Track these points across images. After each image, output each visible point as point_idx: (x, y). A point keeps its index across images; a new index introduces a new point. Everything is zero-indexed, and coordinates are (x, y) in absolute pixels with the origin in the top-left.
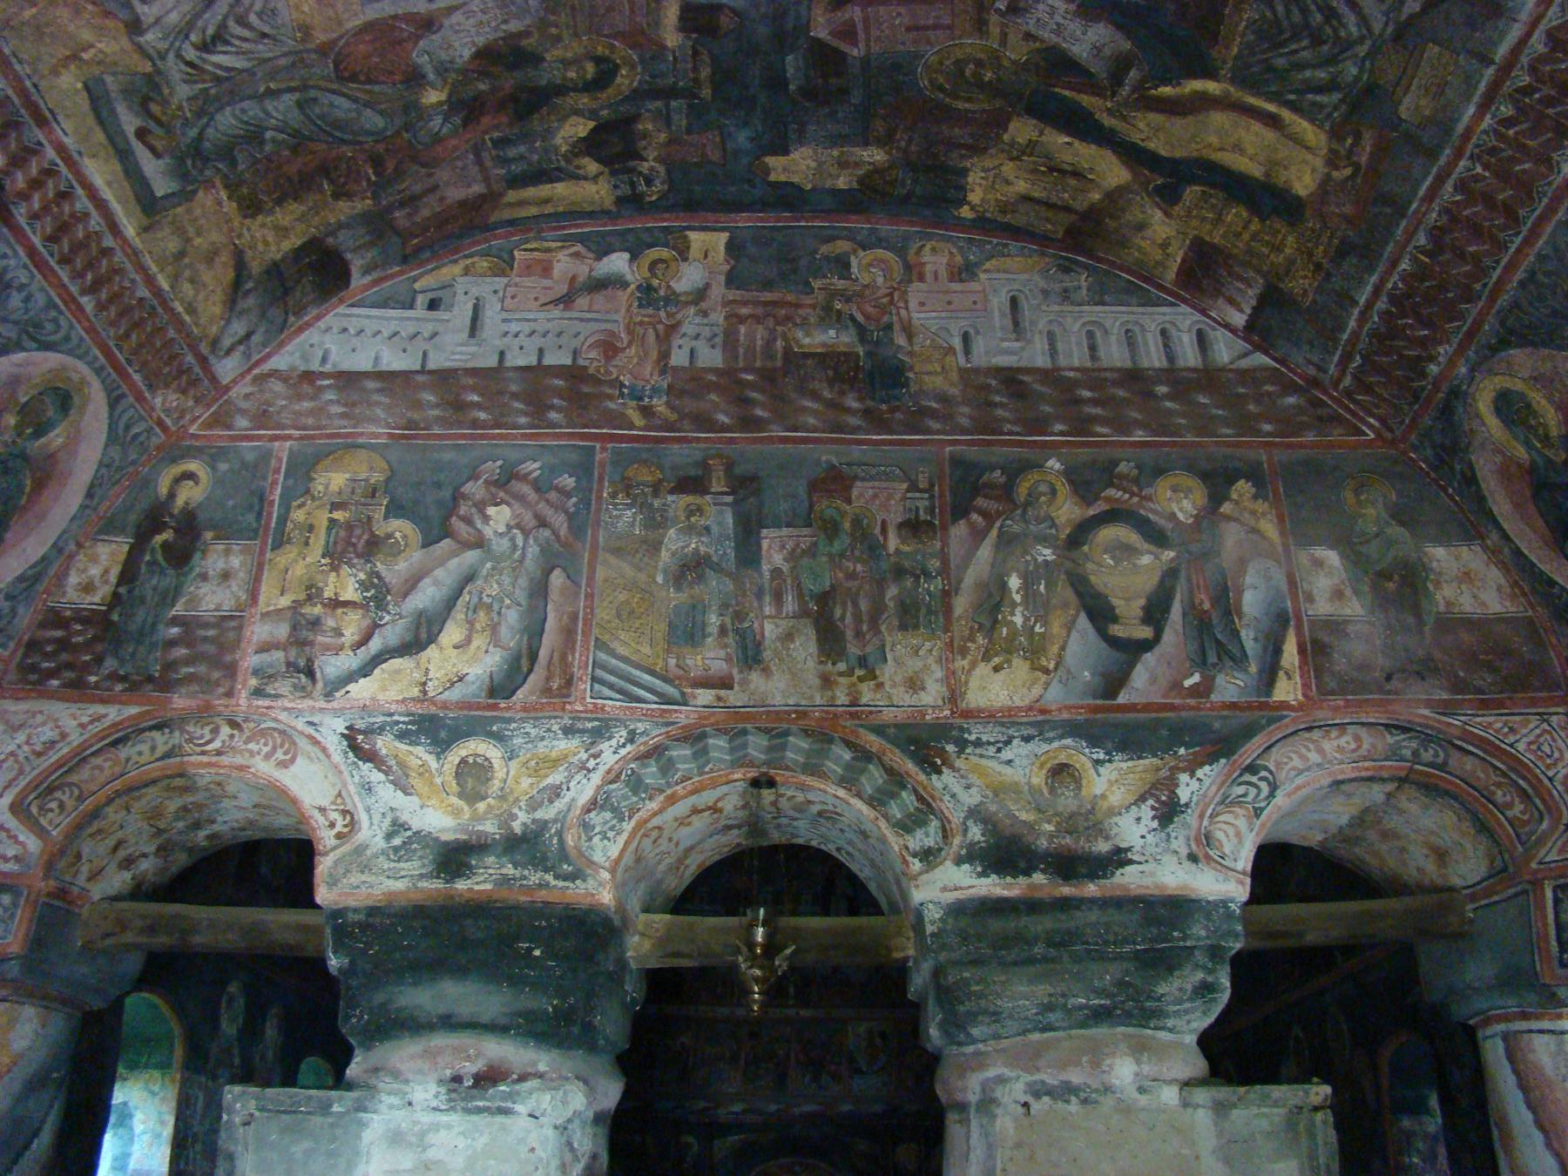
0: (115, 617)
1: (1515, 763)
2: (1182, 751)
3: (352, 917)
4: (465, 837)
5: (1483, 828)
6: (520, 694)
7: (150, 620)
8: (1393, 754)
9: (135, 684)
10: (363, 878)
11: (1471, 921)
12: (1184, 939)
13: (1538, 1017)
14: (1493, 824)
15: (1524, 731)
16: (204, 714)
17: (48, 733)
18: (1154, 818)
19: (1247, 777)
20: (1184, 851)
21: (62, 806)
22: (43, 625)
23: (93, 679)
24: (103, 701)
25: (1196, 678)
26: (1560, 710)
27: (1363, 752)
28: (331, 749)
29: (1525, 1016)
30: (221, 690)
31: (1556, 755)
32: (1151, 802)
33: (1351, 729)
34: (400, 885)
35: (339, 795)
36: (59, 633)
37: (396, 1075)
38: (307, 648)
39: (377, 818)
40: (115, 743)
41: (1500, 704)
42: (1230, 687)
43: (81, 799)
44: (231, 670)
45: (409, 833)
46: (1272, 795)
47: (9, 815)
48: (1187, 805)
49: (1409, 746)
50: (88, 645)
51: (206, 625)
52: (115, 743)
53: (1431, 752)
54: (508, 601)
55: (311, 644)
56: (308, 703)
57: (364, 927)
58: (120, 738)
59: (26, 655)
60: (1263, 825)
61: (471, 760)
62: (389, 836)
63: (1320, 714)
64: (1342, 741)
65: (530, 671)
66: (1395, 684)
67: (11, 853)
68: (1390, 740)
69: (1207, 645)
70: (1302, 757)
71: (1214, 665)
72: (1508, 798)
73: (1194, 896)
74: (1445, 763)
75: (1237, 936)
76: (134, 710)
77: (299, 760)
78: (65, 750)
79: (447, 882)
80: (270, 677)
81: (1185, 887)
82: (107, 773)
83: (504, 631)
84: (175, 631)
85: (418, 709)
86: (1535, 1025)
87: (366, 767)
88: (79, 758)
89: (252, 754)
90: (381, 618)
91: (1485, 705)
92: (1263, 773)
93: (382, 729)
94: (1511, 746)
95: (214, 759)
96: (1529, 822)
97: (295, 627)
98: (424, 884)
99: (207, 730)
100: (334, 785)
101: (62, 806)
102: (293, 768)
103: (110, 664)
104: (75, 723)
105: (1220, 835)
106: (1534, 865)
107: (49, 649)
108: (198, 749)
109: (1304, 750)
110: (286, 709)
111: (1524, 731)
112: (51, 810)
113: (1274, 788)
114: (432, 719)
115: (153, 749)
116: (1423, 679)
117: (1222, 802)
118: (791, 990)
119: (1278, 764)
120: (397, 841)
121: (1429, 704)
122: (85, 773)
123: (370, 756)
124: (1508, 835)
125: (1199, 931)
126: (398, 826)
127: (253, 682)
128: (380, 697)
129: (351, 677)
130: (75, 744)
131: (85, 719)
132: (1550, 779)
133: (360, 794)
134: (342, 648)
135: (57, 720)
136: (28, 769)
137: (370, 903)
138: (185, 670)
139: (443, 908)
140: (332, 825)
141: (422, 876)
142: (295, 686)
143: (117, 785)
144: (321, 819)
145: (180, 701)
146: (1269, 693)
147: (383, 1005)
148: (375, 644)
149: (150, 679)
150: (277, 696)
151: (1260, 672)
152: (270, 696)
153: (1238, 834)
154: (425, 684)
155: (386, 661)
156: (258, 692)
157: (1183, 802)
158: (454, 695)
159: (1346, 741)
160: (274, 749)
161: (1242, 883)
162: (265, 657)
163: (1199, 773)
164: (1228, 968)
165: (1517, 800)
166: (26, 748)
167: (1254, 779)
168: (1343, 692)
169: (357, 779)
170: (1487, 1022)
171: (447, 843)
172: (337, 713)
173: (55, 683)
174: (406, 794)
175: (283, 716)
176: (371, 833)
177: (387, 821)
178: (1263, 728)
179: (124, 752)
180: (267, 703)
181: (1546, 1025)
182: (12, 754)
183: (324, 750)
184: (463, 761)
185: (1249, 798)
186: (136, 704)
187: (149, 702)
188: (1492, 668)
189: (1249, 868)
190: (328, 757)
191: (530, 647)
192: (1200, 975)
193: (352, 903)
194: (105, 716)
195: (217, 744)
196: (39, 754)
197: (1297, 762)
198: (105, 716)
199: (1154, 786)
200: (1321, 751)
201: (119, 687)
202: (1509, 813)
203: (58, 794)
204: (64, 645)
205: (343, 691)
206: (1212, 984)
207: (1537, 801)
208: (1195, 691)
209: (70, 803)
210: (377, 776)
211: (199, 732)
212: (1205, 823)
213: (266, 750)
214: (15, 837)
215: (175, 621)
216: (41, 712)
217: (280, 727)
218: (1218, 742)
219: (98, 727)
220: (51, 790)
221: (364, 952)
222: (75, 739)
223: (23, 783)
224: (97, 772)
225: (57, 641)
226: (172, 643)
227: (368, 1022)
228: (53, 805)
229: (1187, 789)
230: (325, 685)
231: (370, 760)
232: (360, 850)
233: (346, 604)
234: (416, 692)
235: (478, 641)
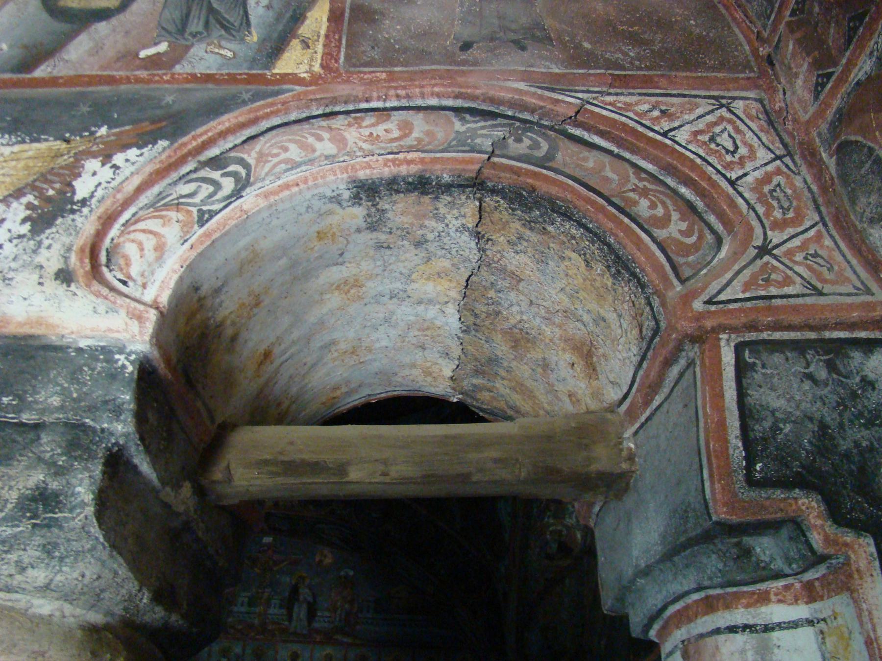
1: (674, 164)
2: (103, 131)
5: (621, 265)
8: (463, 143)
11: (631, 458)
12: (18, 410)
13: (728, 603)
14: (630, 250)
15: (687, 117)
18: (24, 221)
19: (206, 173)
20: (54, 264)
25: (163, 47)
26: (751, 94)
27: (410, 141)
29: (709, 606)
31: (743, 151)
32: (30, 198)
33: (397, 116)
41: (648, 82)
42: (207, 57)
46: (237, 194)
48: (84, 202)
49: (486, 135)
53: (527, 142)
60: (207, 235)
63: (343, 90)
64: (379, 130)
66: (474, 53)
68: (458, 126)
69: (194, 12)
70: (304, 146)
71: (194, 35)
72: (660, 211)
73: (54, 340)
74: (550, 156)
75: (117, 412)
81: (39, 322)
86: (723, 618)
91: (623, 82)
92: (232, 168)
94: (665, 134)
96: (696, 247)
105: (131, 249)
106: (698, 305)
109: (311, 140)
111: (687, 117)
113: (242, 185)
116: (523, 48)
117: (152, 205)
119: (262, 158)
121: (526, 77)
124: (658, 268)
125: (50, 398)
132: (732, 183)
146: (269, 65)
151: (263, 41)
153: (160, 249)
157: (78, 197)
159: (389, 129)
161: (140, 318)
163: (118, 159)
164: (98, 469)
165: (675, 216)
167: (216, 175)
168: (388, 61)
170: (665, 631)
178: (244, 103)
181: (739, 616)
185: (197, 200)
188: (635, 40)
189: (164, 299)
192: (38, 477)
197: (294, 153)
199: (44, 177)
200: (340, 141)
202: (661, 234)
206: (56, 495)
207: (712, 219)
208: (155, 62)
212: (114, 232)
218: (156, 117)
229: (92, 180)
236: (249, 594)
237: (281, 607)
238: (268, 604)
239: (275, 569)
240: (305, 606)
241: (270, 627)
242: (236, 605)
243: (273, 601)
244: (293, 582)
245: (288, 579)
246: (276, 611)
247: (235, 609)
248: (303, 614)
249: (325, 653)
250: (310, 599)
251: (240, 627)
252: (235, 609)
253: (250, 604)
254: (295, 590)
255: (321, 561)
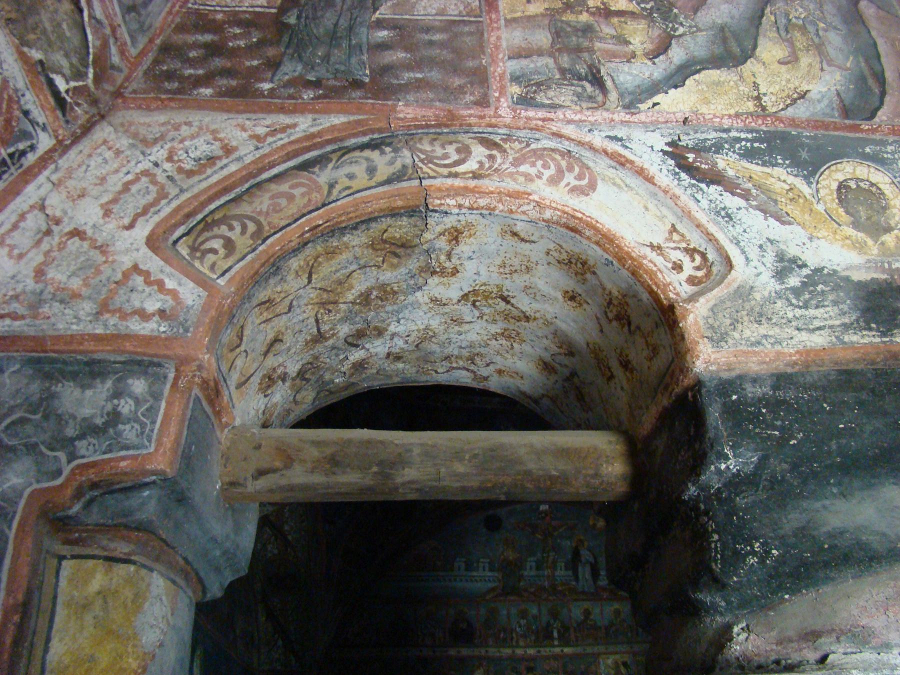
0: (292, 20)
3: (752, 391)
4: (884, 277)
6: (882, 115)
7: (344, 23)
9: (333, 92)
10: (763, 330)
16: (446, 128)
17: (202, 147)
21: (229, 245)
22: (181, 28)
23: (266, 86)
24: (282, 110)
28: (653, 170)
30: (469, 98)
34: (819, 340)
35: (674, 229)
36: (208, 38)
37: (861, 637)
38: (585, 55)
39: (754, 253)
40: (305, 166)
43: (260, 236)
44: (480, 77)
45: (805, 271)
47: (145, 250)
50: (251, 50)
51: (428, 30)
52: (305, 166)
54: (822, 25)
55: (591, 51)
56: (599, 116)
57: (775, 405)
58: (311, 158)
59: (156, 62)
61: (853, 185)
62: (780, 275)
65: (883, 94)
67: (152, 306)
76: (338, 120)
77: (600, 185)
78: (233, 168)
79: (884, 334)
80: (539, 84)
82: (300, 202)
83: (831, 51)
84: (383, 34)
85: (763, 126)
87: (714, 190)
88: (252, 182)
89: (529, 178)
90: (675, 30)
93: (718, 147)
95: (472, 183)
97: (557, 34)
98: (852, 338)
99: (451, 149)
100: (662, 218)
101: (229, 245)
102: (594, 195)
103: (291, 69)
104: (245, 135)
107: (193, 54)
108: (445, 171)
110: (570, 122)
112: (214, 251)
114: (784, 137)
115: (371, 171)
118: (555, 634)
120: (794, 281)
122: (262, 203)
123: (715, 178)
126: (786, 265)
127: (515, 90)
128: (704, 109)
129: (655, 88)
130: (248, 160)
131: (261, 131)
133: (717, 223)
134: (634, 55)
135: (214, 132)
136: (173, 191)
137: (780, 366)
138: (407, 76)
139: (879, 374)
140: (678, 267)
141: (846, 327)
142: (579, 96)
143: (317, 218)
144: (659, 260)
145: (407, 110)
147: (802, 532)
148: (677, 54)
149: (357, 84)
150: (554, 107)
152: (543, 106)
154: (758, 98)
155: (698, 72)
156: (526, 101)
158: (801, 111)
160: (560, 173)
162: (524, 62)
166: (167, 166)
169: (704, 203)
171: (861, 285)
172: (651, 126)
173: (208, 91)
174: (783, 223)
175: (569, 130)
176: (753, 272)
177: (770, 258)
179: (323, 177)
180: (541, 114)
182: (146, 173)
183: (641, 172)
184: (842, 187)
186: (339, 112)
187: (359, 110)
190: (650, 180)
191: (871, 69)
193: (753, 366)
194: (295, 125)
195: (471, 165)
196: (190, 174)
198: (295, 125)
201: (308, 95)
203: (224, 230)
204: (213, 50)
205: (650, 103)
209: (242, 242)
210: (732, 202)
211: (439, 152)
213: (547, 173)
214: (160, 284)
215: (380, 24)
216: (189, 124)
217: (566, 145)
219: (283, 139)
220: (207, 224)
221: (782, 442)
222: (248, 153)
223: (167, 210)
224: (283, 202)
225: (206, 46)
226: (383, 46)
227: (781, 561)
228: (217, 244)
230: (621, 96)
231: (718, 183)
232: (743, 293)
233: (621, 13)
234: (750, 106)
235: (805, 60)
236: (535, 559)
237: (566, 569)
238: (554, 568)
239: (556, 534)
240: (588, 568)
241: (560, 588)
242: (526, 570)
243: (559, 564)
244: (574, 545)
245: (569, 543)
246: (563, 573)
247: (526, 573)
248: (588, 576)
249: (612, 609)
250: (592, 560)
251: (532, 590)
252: (526, 573)
253: (538, 569)
254: (576, 554)
255: (595, 525)
